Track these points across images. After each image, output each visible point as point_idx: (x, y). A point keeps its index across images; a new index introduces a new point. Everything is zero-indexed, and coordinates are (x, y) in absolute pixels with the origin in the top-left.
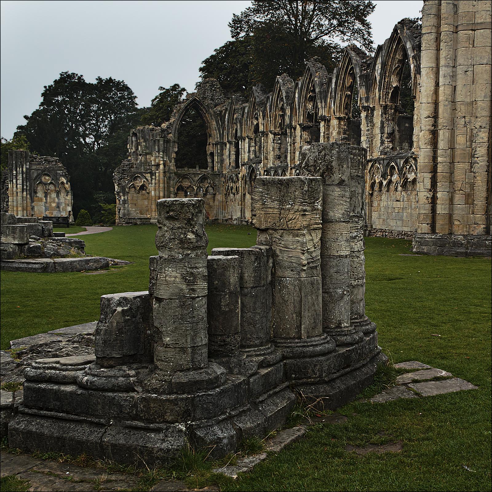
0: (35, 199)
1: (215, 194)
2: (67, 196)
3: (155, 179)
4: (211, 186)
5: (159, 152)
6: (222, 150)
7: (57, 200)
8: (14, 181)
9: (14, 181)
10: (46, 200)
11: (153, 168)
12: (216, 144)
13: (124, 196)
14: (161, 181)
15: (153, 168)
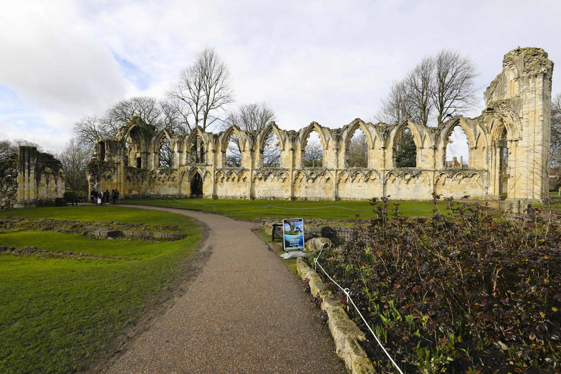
0: (40, 184)
1: (143, 181)
2: (62, 182)
3: (117, 172)
4: (141, 177)
5: (120, 155)
6: (147, 156)
7: (55, 186)
8: (26, 171)
9: (26, 171)
10: (47, 185)
11: (115, 165)
12: (144, 153)
13: (98, 182)
14: (122, 173)
15: (115, 165)
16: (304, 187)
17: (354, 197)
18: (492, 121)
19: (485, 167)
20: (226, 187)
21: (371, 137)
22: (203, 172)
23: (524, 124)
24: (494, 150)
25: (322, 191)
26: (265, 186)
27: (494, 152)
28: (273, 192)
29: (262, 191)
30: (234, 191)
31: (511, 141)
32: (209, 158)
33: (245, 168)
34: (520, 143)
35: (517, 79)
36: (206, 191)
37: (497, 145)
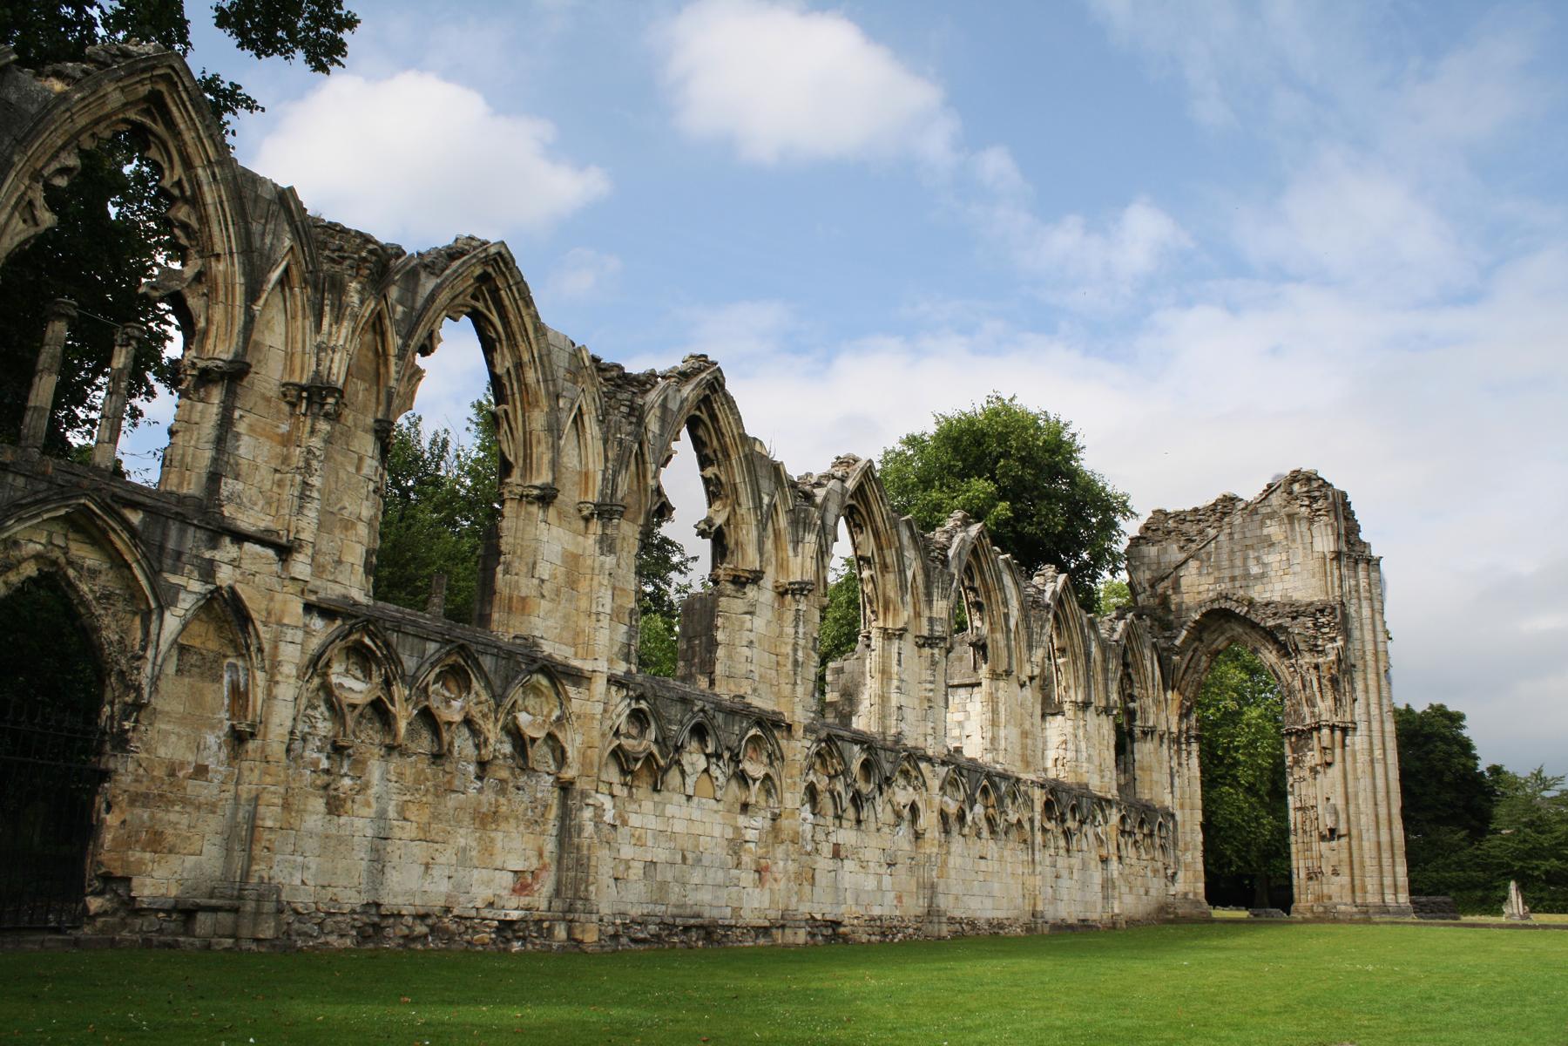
16: (826, 849)
17: (969, 914)
18: (1190, 654)
19: (1168, 800)
20: (382, 815)
21: (1007, 616)
22: (166, 598)
23: (1359, 686)
24: (1184, 747)
25: (887, 880)
26: (653, 823)
27: (1184, 754)
28: (696, 877)
29: (637, 870)
30: (447, 856)
31: (1332, 728)
32: (247, 448)
33: (547, 648)
34: (1348, 740)
35: (1338, 556)
36: (156, 841)
37: (1193, 733)
